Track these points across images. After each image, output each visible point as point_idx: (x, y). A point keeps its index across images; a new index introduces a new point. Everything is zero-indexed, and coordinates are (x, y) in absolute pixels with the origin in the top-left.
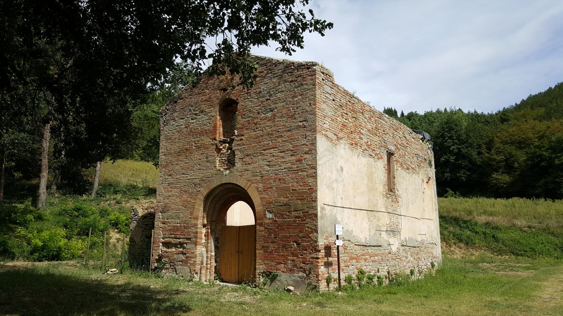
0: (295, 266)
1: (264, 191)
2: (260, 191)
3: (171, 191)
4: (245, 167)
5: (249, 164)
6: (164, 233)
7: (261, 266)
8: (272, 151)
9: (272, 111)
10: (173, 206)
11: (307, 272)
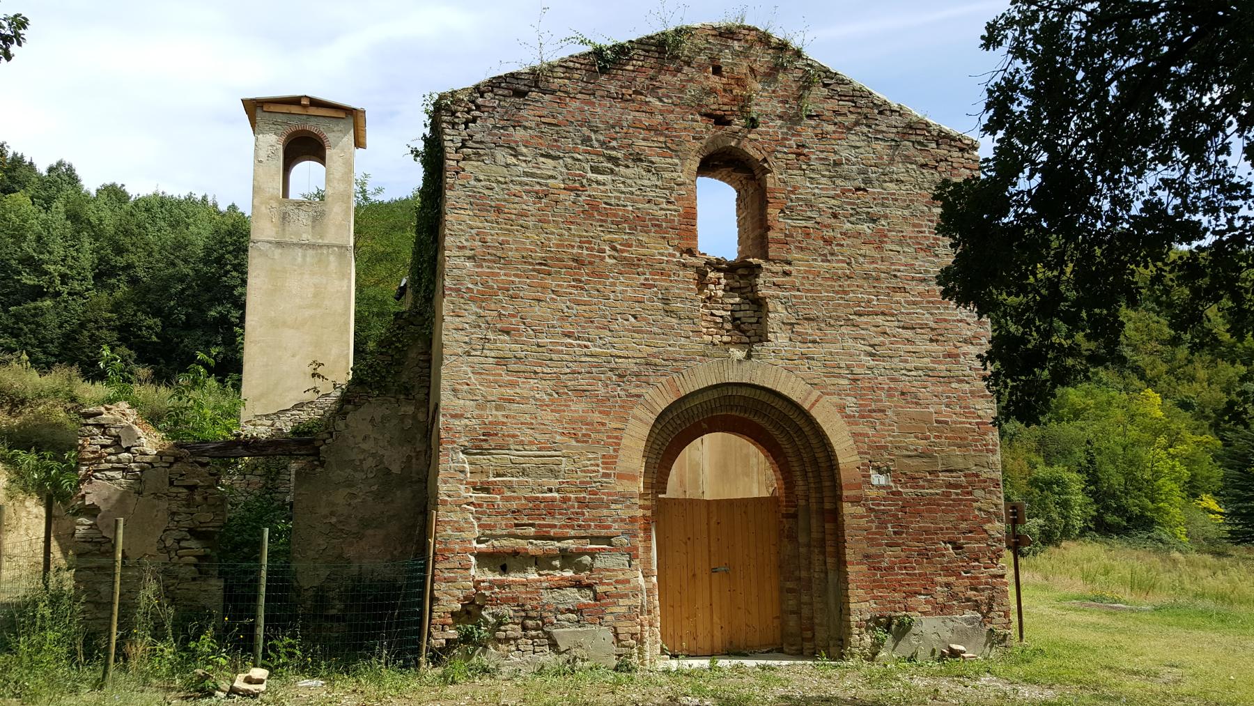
0: (954, 596)
1: (863, 417)
2: (848, 416)
3: (512, 384)
4: (800, 348)
5: (814, 342)
6: (485, 520)
7: (864, 605)
8: (879, 320)
9: (874, 221)
10: (526, 435)
11: (984, 608)
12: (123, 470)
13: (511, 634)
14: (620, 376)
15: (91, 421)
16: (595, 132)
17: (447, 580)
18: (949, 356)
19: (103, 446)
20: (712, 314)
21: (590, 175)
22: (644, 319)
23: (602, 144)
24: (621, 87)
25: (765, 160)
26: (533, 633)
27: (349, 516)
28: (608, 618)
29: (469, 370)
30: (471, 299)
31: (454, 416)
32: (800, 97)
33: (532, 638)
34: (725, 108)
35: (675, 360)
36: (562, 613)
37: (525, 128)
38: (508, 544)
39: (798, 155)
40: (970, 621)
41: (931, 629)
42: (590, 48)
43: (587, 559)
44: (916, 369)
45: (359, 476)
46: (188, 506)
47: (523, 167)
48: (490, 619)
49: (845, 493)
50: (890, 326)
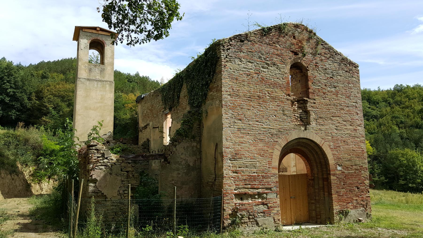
0: (358, 203)
1: (335, 149)
2: (331, 149)
3: (242, 137)
4: (319, 127)
5: (322, 125)
6: (237, 183)
7: (337, 207)
8: (338, 118)
9: (335, 88)
10: (247, 154)
11: (365, 206)
12: (105, 165)
13: (246, 221)
14: (272, 135)
15: (94, 148)
16: (263, 55)
17: (227, 203)
18: (355, 130)
19: (98, 157)
20: (295, 115)
21: (261, 69)
22: (278, 117)
23: (265, 59)
24: (269, 41)
25: (307, 67)
26: (252, 220)
27: (178, 181)
28: (272, 214)
29: (230, 132)
30: (230, 109)
31: (227, 148)
32: (316, 48)
33: (251, 222)
34: (297, 49)
35: (287, 130)
36: (259, 213)
37: (244, 52)
38: (243, 191)
39: (316, 66)
40: (362, 211)
41: (353, 213)
42: (260, 28)
43: (265, 195)
44: (347, 134)
45: (181, 167)
46: (127, 178)
47: (243, 65)
48: (239, 216)
49: (331, 173)
50: (340, 120)
